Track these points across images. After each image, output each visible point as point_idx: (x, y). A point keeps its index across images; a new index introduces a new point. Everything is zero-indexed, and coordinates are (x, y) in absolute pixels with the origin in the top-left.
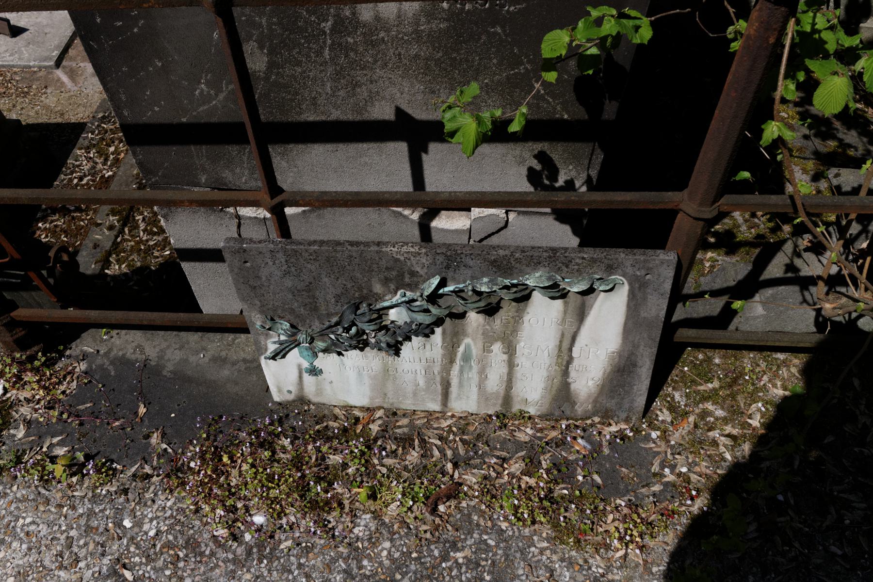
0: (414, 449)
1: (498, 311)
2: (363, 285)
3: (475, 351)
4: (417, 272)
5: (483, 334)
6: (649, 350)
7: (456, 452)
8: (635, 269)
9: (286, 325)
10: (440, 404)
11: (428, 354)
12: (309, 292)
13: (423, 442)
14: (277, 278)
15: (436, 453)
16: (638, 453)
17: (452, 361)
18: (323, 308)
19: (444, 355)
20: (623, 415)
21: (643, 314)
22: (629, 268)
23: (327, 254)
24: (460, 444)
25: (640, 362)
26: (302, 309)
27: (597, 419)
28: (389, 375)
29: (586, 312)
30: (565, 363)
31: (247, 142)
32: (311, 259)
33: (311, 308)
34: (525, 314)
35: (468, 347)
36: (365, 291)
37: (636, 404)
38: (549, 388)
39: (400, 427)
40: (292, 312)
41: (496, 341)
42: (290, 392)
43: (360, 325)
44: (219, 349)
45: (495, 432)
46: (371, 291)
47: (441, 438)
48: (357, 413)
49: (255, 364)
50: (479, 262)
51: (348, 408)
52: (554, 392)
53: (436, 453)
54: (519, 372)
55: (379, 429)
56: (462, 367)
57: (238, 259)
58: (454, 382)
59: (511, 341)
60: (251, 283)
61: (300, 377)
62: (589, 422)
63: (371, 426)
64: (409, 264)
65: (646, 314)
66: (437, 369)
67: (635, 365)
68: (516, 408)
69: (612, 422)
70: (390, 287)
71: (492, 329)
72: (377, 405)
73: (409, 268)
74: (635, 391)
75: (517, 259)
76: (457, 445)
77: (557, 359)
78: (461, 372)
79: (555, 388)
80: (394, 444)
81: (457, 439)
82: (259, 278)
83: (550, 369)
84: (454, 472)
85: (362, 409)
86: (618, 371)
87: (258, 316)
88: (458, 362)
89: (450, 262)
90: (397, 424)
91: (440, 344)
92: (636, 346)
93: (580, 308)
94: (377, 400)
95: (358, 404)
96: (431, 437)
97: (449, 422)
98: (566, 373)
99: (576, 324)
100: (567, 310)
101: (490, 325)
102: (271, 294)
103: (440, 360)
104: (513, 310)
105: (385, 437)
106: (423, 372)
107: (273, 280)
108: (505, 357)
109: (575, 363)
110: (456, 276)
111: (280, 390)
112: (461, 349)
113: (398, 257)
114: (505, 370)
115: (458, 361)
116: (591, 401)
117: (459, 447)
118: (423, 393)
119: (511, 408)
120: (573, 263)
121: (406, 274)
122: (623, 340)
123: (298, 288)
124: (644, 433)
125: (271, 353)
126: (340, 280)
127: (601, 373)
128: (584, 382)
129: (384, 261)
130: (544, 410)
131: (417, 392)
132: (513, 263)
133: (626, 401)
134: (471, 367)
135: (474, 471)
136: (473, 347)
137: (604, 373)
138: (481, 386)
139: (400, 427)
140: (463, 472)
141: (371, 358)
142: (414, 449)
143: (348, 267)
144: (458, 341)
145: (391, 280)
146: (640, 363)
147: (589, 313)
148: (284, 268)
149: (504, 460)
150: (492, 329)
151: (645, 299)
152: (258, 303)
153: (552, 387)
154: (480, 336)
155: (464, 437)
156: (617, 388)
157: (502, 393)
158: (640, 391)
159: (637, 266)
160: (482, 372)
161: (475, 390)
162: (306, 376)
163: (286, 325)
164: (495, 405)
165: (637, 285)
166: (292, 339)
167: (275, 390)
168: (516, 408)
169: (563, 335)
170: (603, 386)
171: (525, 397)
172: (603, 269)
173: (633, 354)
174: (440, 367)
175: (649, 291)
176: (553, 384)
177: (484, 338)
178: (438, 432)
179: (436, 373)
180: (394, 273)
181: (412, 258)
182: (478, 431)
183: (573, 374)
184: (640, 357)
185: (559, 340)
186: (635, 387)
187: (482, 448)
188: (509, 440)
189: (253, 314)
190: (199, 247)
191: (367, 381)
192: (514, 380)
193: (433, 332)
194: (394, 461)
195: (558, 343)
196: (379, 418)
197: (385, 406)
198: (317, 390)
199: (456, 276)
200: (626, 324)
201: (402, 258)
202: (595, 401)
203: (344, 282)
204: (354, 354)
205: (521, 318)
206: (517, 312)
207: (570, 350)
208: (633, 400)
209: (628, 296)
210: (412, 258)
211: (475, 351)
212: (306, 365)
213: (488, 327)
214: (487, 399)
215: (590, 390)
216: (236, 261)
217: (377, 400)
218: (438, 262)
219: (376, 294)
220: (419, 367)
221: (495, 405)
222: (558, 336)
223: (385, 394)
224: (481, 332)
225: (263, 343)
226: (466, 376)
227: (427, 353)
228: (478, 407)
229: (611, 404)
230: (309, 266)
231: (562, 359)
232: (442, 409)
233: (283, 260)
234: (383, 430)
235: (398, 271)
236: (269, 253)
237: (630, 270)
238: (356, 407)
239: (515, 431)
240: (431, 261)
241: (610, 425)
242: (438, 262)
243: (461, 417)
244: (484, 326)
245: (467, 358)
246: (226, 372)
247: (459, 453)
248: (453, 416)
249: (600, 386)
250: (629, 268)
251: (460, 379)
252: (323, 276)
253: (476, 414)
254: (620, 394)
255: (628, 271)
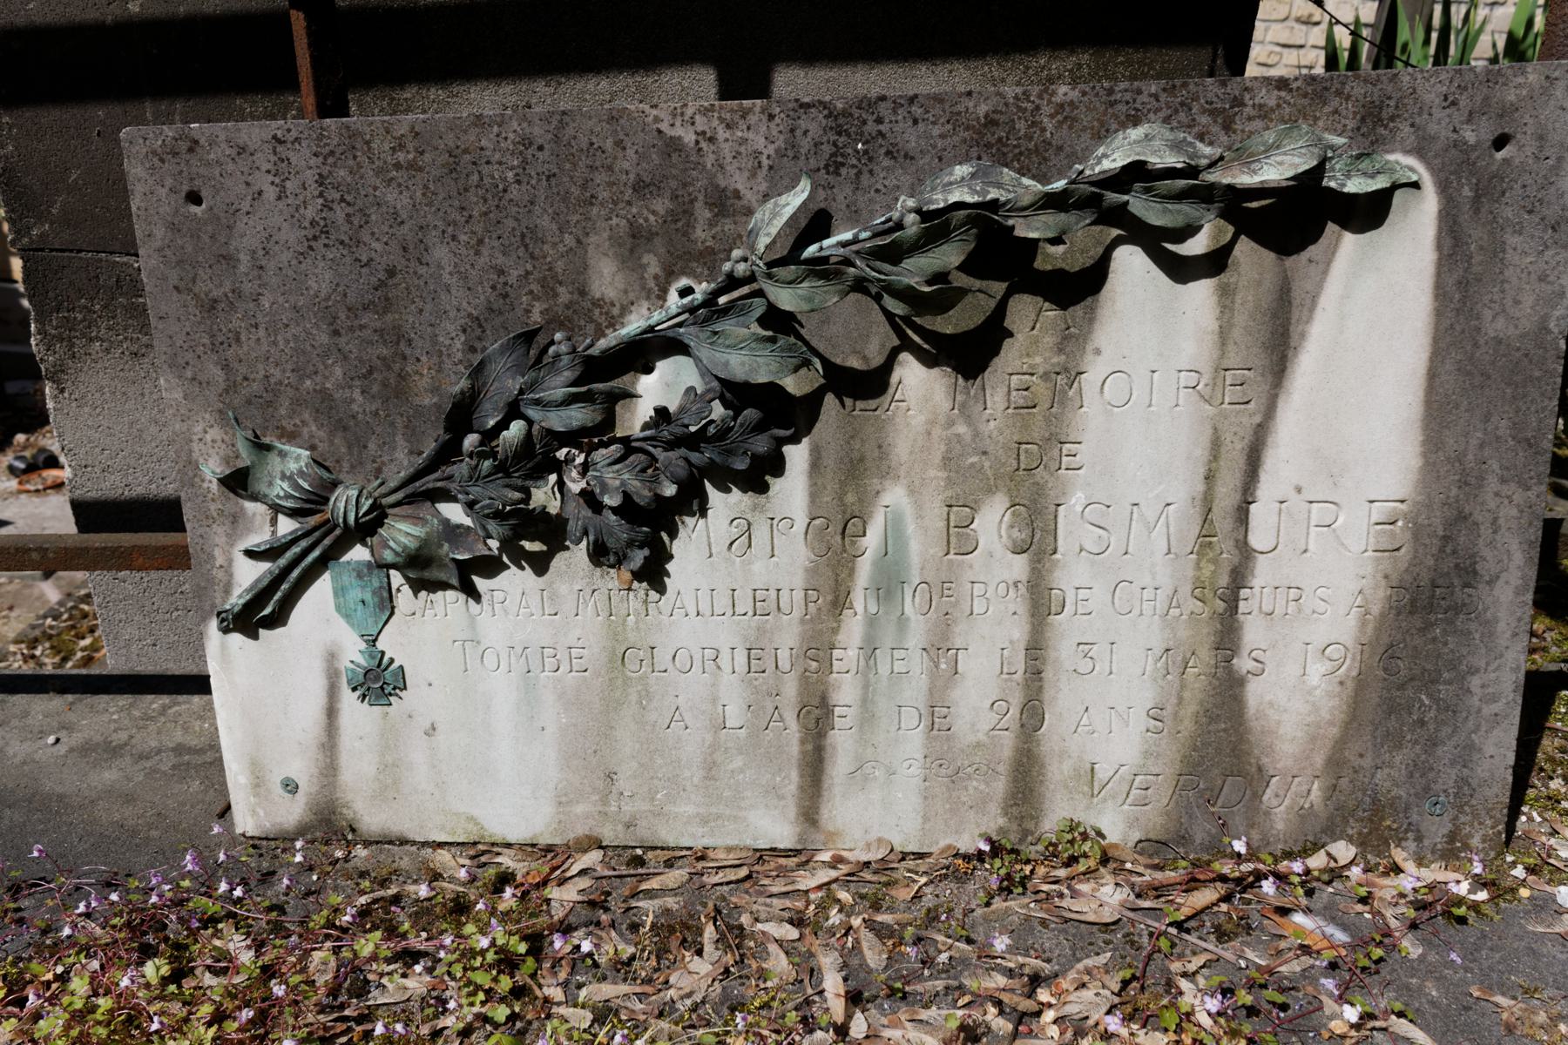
0: (699, 953)
1: (995, 351)
2: (560, 266)
3: (920, 548)
4: (737, 195)
5: (947, 461)
6: (1519, 496)
7: (855, 962)
8: (1458, 116)
9: (298, 458)
10: (792, 811)
11: (761, 571)
12: (386, 311)
13: (734, 936)
14: (286, 257)
15: (779, 963)
16: (1532, 952)
17: (839, 602)
18: (424, 383)
19: (812, 572)
20: (1437, 830)
21: (1495, 327)
22: (1438, 113)
23: (450, 140)
24: (867, 938)
25: (1486, 552)
26: (357, 394)
27: (1343, 851)
28: (627, 682)
29: (1294, 330)
30: (1224, 580)
31: (294, 87)
32: (398, 166)
33: (385, 385)
34: (1089, 357)
35: (894, 529)
36: (564, 295)
37: (1482, 770)
38: (1169, 709)
39: (650, 894)
40: (324, 404)
41: (990, 491)
42: (291, 787)
43: (532, 413)
44: (112, 726)
45: (988, 904)
46: (583, 293)
47: (798, 921)
48: (507, 861)
49: (209, 757)
50: (936, 131)
51: (479, 850)
52: (1188, 726)
53: (779, 963)
54: (1067, 631)
55: (580, 898)
56: (872, 621)
57: (169, 182)
58: (845, 693)
59: (1039, 490)
60: (200, 287)
61: (331, 712)
62: (1317, 861)
63: (553, 892)
64: (709, 160)
65: (1500, 323)
66: (787, 637)
67: (1468, 573)
68: (1056, 813)
69: (1399, 855)
70: (644, 267)
71: (976, 434)
72: (580, 830)
73: (712, 177)
74: (1475, 701)
75: (1061, 106)
76: (857, 941)
77: (1198, 567)
78: (870, 650)
79: (1191, 709)
80: (627, 942)
81: (856, 922)
82: (229, 259)
83: (1174, 612)
84: (849, 1017)
85: (530, 849)
86: (1413, 607)
87: (215, 433)
88: (859, 606)
89: (842, 140)
90: (644, 886)
91: (801, 522)
92: (1470, 482)
93: (1275, 316)
94: (580, 809)
95: (516, 832)
96: (763, 916)
97: (825, 875)
98: (1227, 634)
99: (1257, 391)
100: (1231, 325)
101: (969, 420)
102: (261, 333)
103: (799, 595)
104: (1049, 340)
105: (598, 924)
106: (741, 658)
107: (271, 266)
108: (1019, 566)
109: (1263, 574)
110: (862, 200)
111: (258, 783)
112: (872, 540)
113: (678, 131)
114: (1018, 631)
115: (858, 599)
116: (1319, 760)
117: (865, 945)
118: (738, 762)
119: (1036, 819)
120: (1248, 110)
121: (699, 205)
122: (1424, 455)
123: (352, 299)
124: (1524, 893)
125: (240, 597)
126: (485, 251)
127: (1352, 621)
128: (1293, 670)
129: (630, 152)
130: (1154, 820)
131: (719, 757)
132: (1049, 124)
133: (1445, 751)
134: (902, 621)
135: (924, 1015)
136: (911, 528)
137: (1363, 624)
138: (936, 717)
139: (650, 894)
140: (885, 1021)
141: (568, 606)
142: (699, 953)
143: (514, 192)
144: (860, 500)
145: (651, 236)
146: (1486, 568)
147: (1303, 336)
148: (310, 213)
149: (1036, 980)
150: (976, 434)
151: (1496, 251)
152: (218, 374)
153: (1180, 700)
154: (936, 474)
155: (880, 918)
156: (1410, 692)
157: (1007, 743)
158: (1494, 699)
159: (1464, 101)
160: (941, 648)
161: (913, 741)
162: (349, 700)
163: (298, 458)
164: (980, 805)
165: (1467, 192)
166: (312, 521)
167: (243, 780)
168: (1056, 813)
169: (1216, 445)
170: (1361, 683)
171: (1090, 758)
172: (1351, 124)
173: (1462, 517)
174: (796, 629)
175: (1508, 213)
176: (1183, 686)
177: (950, 482)
178: (788, 903)
179: (785, 664)
180: (661, 205)
181: (722, 134)
182: (928, 901)
183: (1253, 633)
184: (1486, 531)
185: (1202, 471)
186: (1475, 682)
187: (946, 950)
188: (1043, 922)
189: (199, 428)
190: (138, 491)
191: (551, 715)
192: (1048, 674)
193: (777, 466)
194: (624, 988)
195: (1200, 487)
196: (583, 872)
197: (609, 835)
198: (384, 768)
199: (862, 200)
200: (1432, 375)
201: (689, 137)
202: (1335, 763)
203: (500, 260)
204: (515, 581)
205: (1074, 375)
206: (1061, 351)
207: (1242, 515)
208: (1470, 747)
209: (1439, 246)
210: (722, 134)
211: (920, 548)
212: (353, 652)
213: (961, 429)
214: (956, 778)
215: (1316, 709)
216: (163, 192)
217: (580, 809)
218: (805, 144)
219: (598, 303)
220: (727, 635)
221: (980, 805)
222: (1201, 452)
223: (610, 776)
224: (939, 451)
225: (220, 561)
226: (884, 669)
227: (757, 567)
228: (926, 819)
229: (1390, 778)
230: (391, 196)
231: (1215, 561)
232: (801, 840)
233: (310, 176)
234: (592, 904)
235: (674, 197)
236: (268, 148)
237: (1439, 125)
238: (509, 846)
239: (1061, 896)
240: (780, 143)
241: (1397, 870)
242: (805, 144)
243: (867, 864)
244: (951, 423)
245: (888, 586)
246: (109, 775)
247: (863, 964)
248: (837, 861)
249: (1350, 685)
250: (1438, 113)
251: (866, 686)
252: (433, 237)
253: (921, 856)
254: (1422, 723)
255: (1433, 128)
